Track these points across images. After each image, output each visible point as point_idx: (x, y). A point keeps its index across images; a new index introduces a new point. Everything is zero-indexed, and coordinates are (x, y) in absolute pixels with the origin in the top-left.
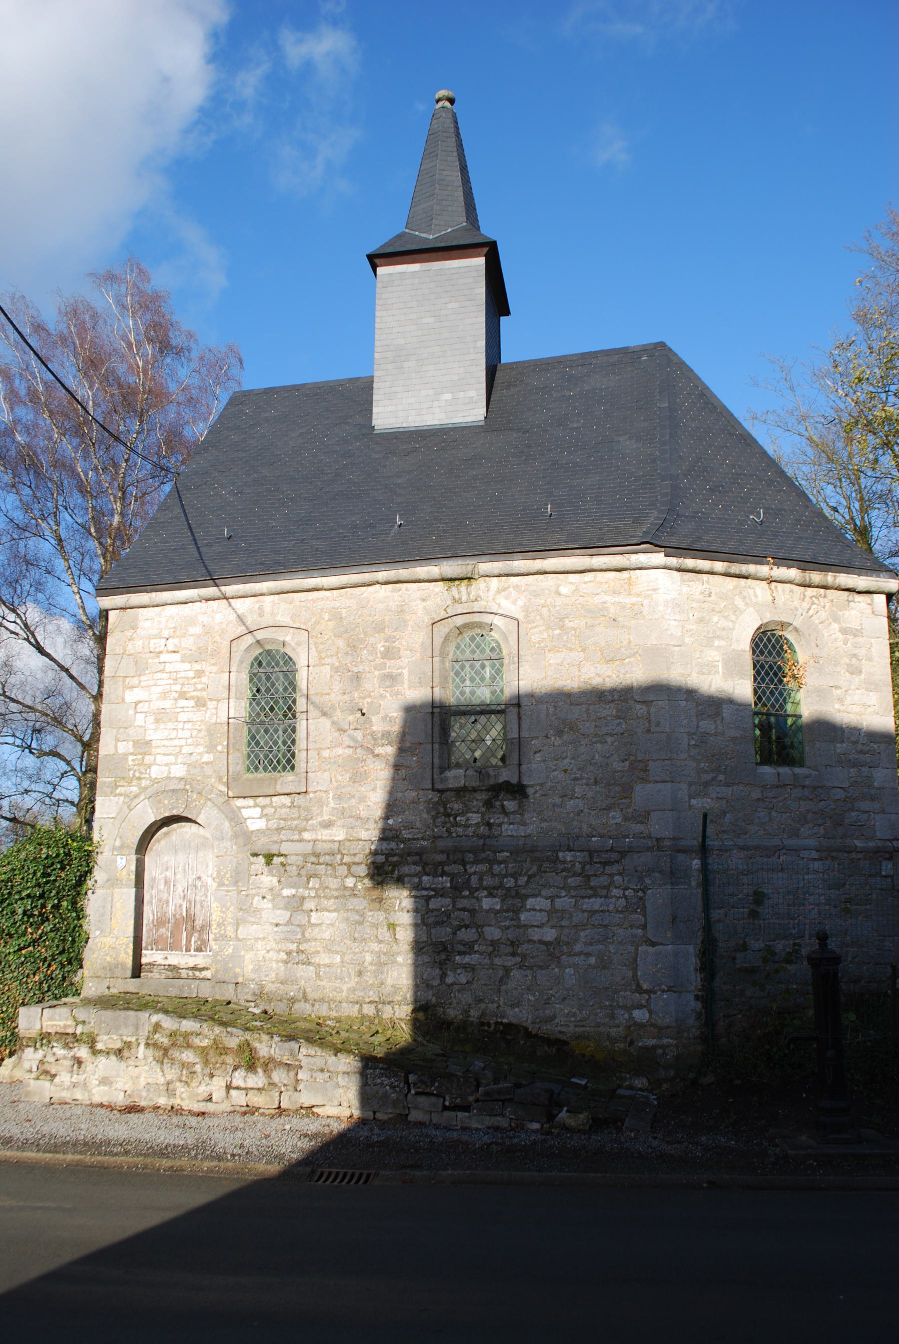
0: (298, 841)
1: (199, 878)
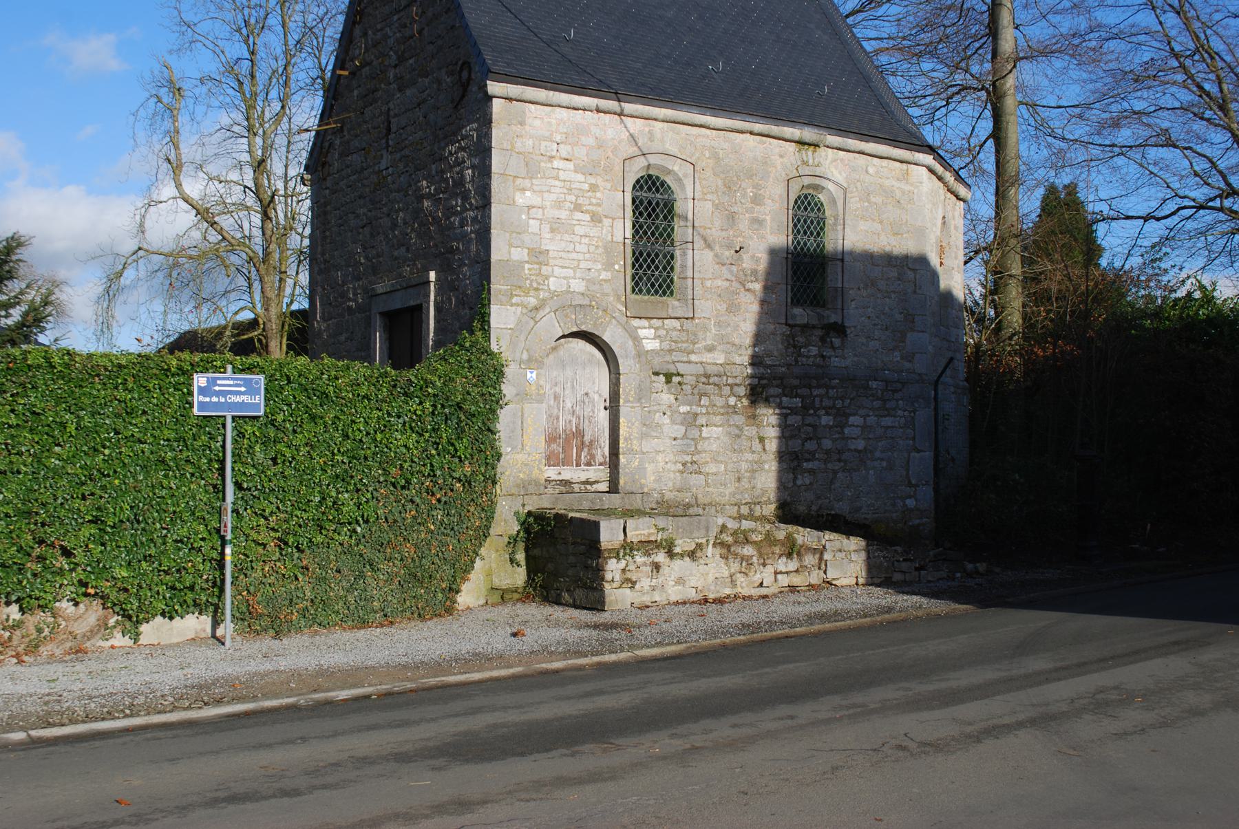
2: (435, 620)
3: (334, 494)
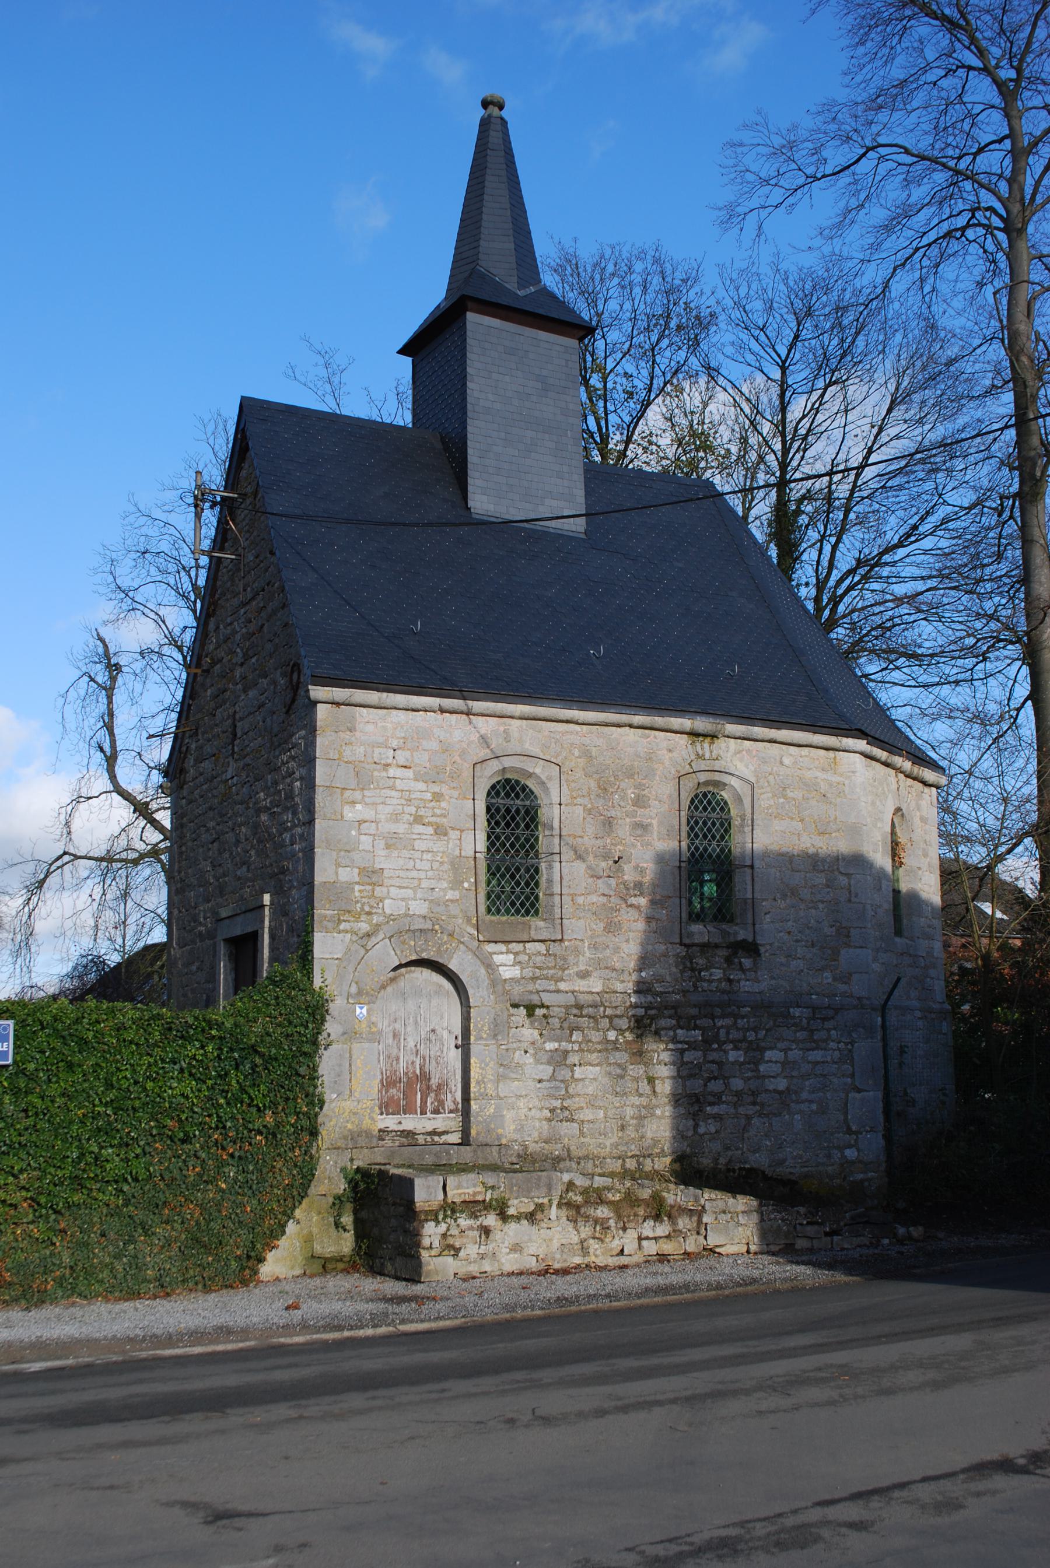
1: (433, 1031)
2: (224, 1291)
3: (96, 1149)
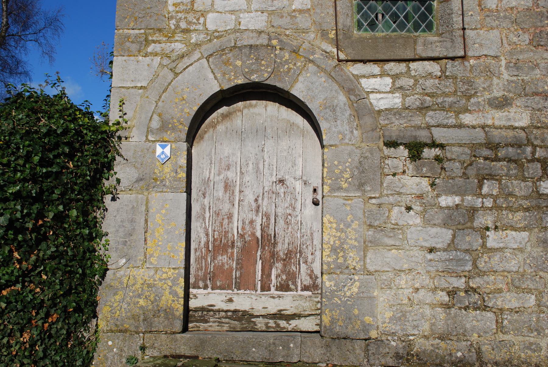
0: (455, 126)
1: (282, 181)
